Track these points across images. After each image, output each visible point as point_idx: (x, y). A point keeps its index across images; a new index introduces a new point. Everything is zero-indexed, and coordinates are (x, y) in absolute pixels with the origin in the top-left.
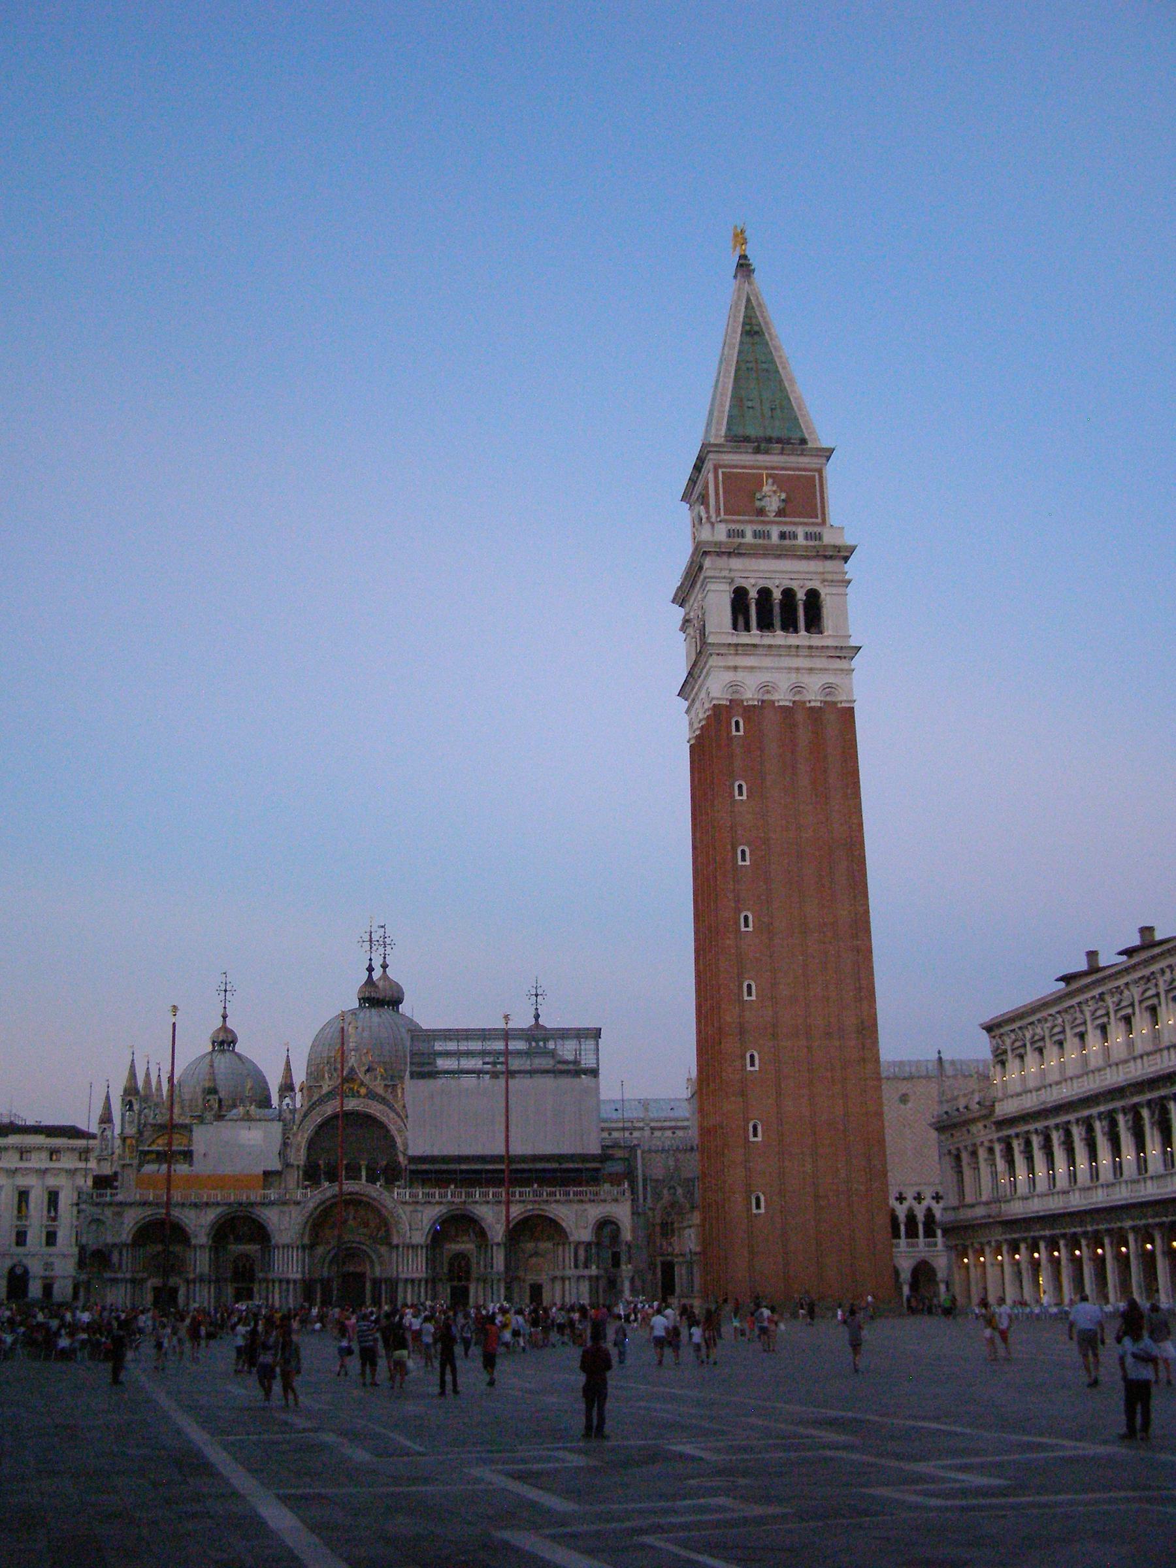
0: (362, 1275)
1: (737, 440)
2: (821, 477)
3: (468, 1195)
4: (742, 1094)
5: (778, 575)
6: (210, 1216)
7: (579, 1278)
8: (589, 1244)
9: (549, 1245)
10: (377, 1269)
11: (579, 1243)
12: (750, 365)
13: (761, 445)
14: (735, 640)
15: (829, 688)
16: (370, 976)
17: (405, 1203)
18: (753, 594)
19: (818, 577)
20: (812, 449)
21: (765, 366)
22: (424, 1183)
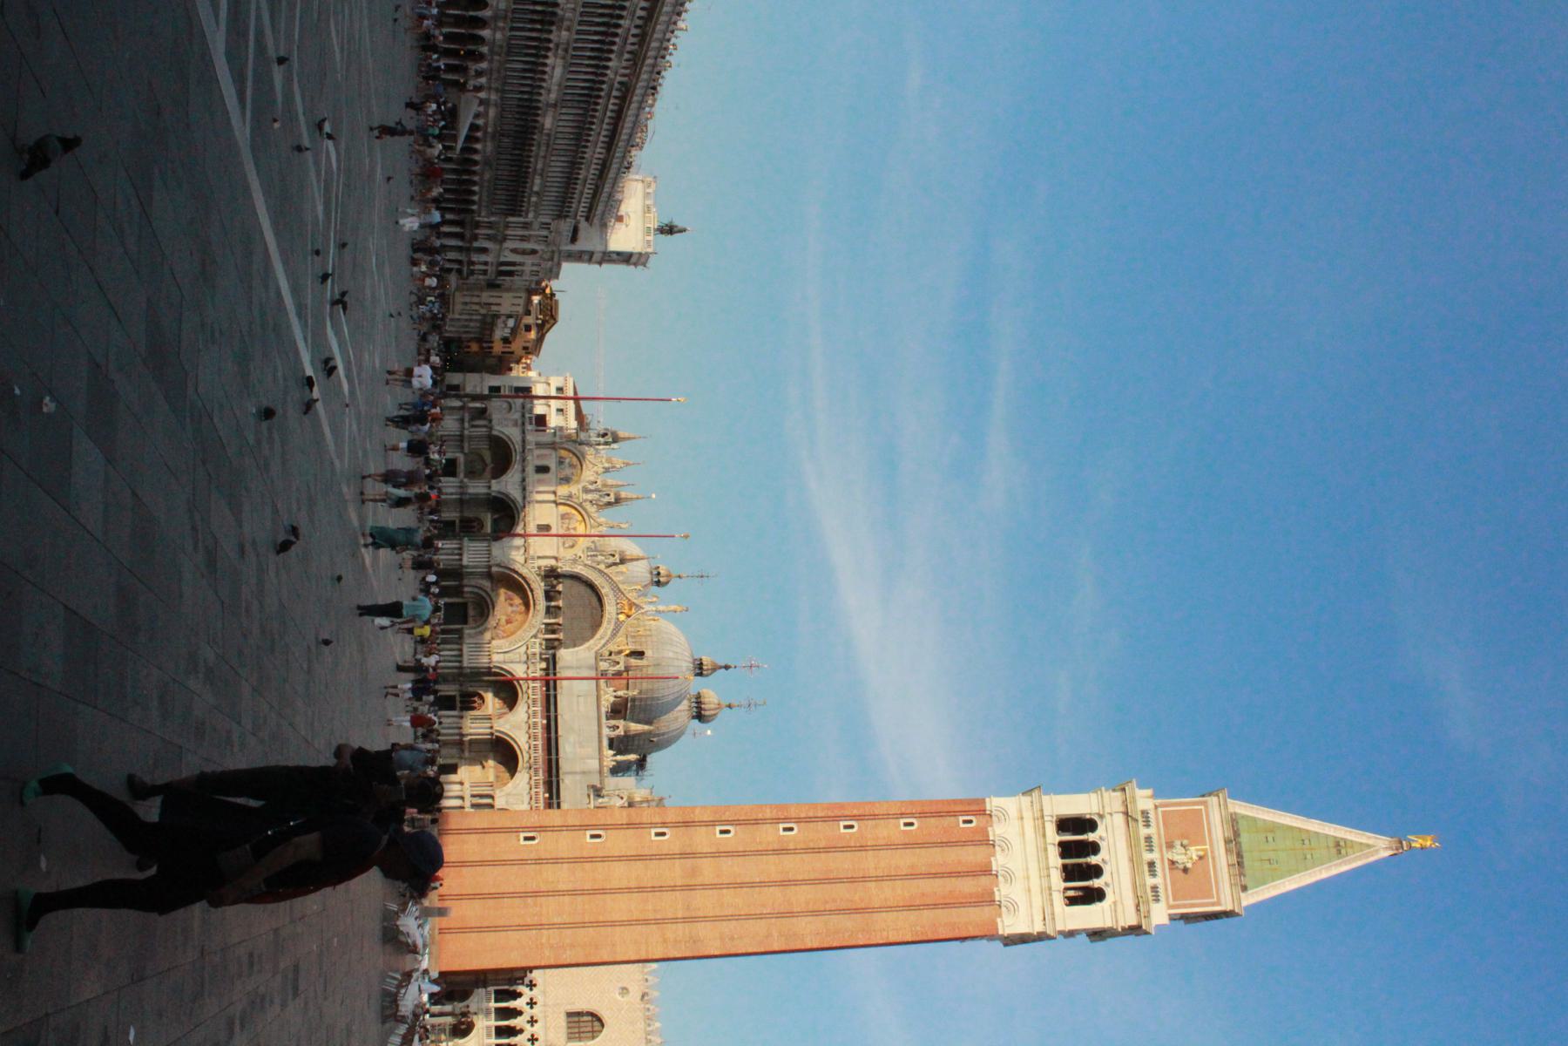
0: (465, 622)
1: (1234, 821)
2: (1213, 904)
3: (534, 701)
4: (630, 825)
6: (515, 493)
9: (492, 779)
11: (492, 797)
13: (1233, 842)
15: (1014, 907)
18: (1091, 837)
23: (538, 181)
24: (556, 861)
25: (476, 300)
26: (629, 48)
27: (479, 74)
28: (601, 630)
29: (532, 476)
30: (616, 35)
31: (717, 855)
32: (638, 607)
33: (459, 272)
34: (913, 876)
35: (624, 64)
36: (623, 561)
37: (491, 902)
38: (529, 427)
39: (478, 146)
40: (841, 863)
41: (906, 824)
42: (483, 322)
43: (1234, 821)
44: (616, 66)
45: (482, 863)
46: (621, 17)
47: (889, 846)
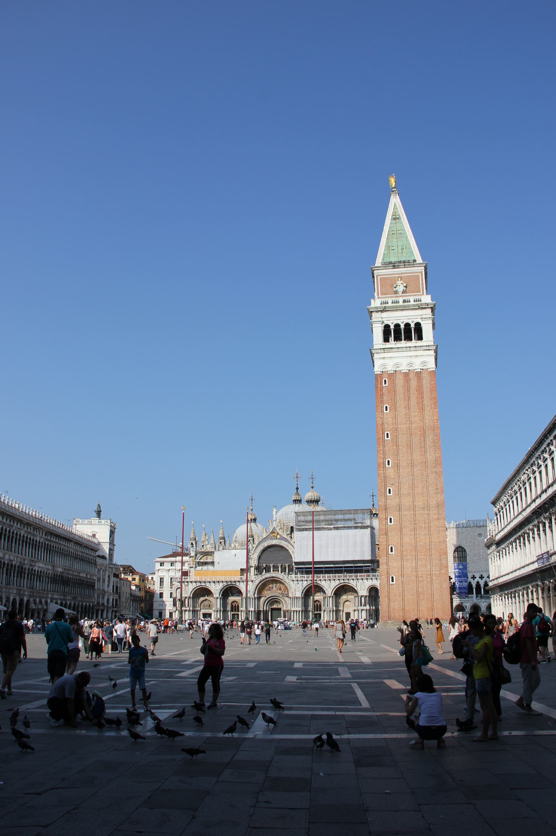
2: (422, 275)
3: (317, 577)
5: (403, 318)
6: (220, 586)
7: (362, 610)
8: (366, 596)
11: (362, 596)
12: (394, 232)
13: (394, 265)
16: (297, 491)
17: (293, 581)
18: (392, 327)
19: (420, 317)
20: (418, 264)
21: (400, 232)
22: (302, 573)
23: (82, 575)
24: (402, 567)
25: (124, 603)
26: (32, 531)
27: (41, 602)
28: (285, 546)
30: (27, 537)
31: (399, 495)
33: (116, 612)
34: (408, 407)
35: (38, 533)
36: (252, 536)
37: (421, 596)
38: (188, 580)
39: (68, 602)
40: (403, 440)
41: (386, 410)
42: (133, 601)
44: (39, 537)
45: (403, 600)
46: (20, 535)
47: (395, 418)
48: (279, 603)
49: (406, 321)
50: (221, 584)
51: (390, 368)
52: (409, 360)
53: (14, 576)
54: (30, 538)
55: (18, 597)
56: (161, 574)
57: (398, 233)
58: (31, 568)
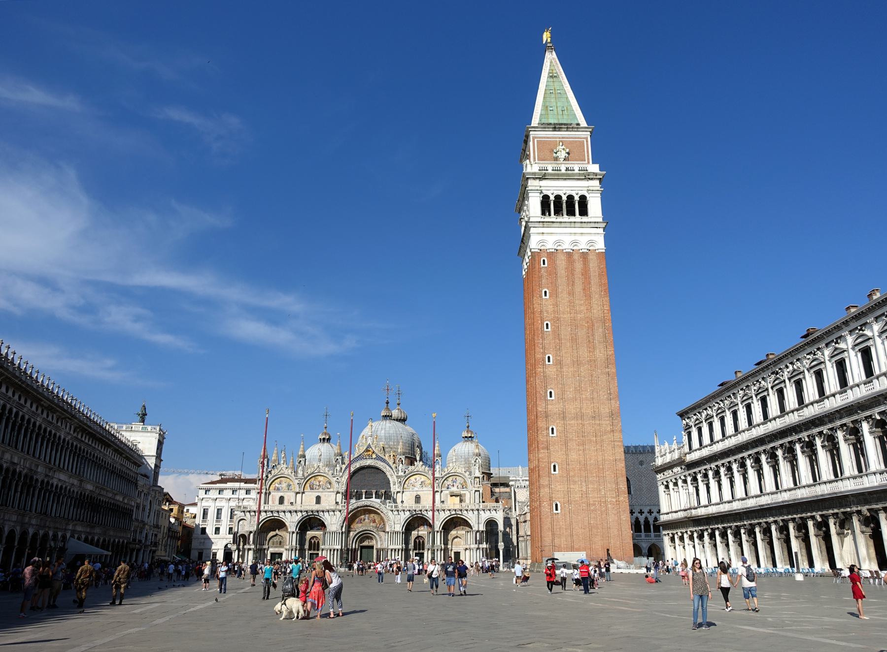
0: (372, 547)
6: (298, 517)
10: (379, 543)
13: (556, 127)
14: (542, 220)
15: (591, 242)
18: (552, 198)
24: (569, 492)
26: (55, 421)
27: (55, 536)
28: (381, 467)
29: (286, 506)
30: (45, 429)
32: (369, 446)
35: (64, 426)
36: (341, 455)
39: (96, 538)
40: (565, 332)
41: (546, 295)
43: (544, 126)
44: (65, 432)
46: (35, 423)
47: (556, 305)
48: (372, 539)
49: (569, 193)
50: (300, 514)
51: (550, 246)
52: (573, 238)
53: (16, 491)
54: (50, 432)
55: (18, 528)
56: (205, 504)
57: (554, 93)
58: (46, 480)
